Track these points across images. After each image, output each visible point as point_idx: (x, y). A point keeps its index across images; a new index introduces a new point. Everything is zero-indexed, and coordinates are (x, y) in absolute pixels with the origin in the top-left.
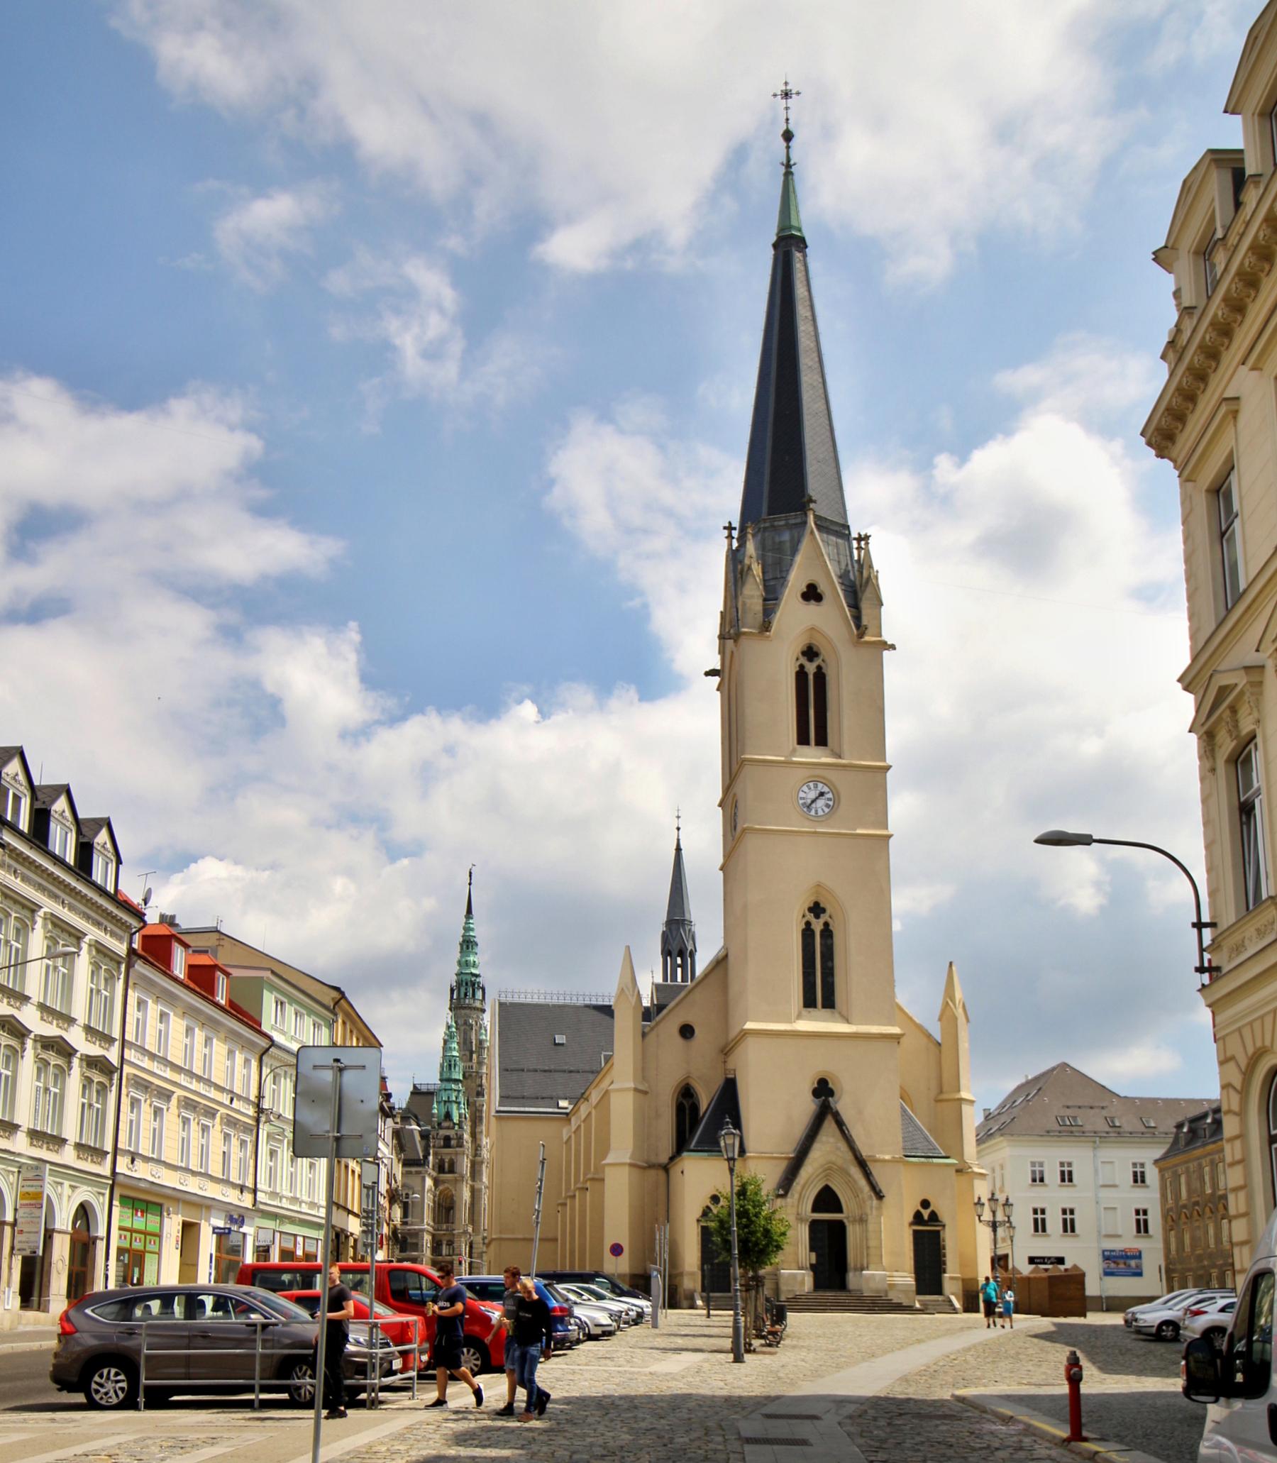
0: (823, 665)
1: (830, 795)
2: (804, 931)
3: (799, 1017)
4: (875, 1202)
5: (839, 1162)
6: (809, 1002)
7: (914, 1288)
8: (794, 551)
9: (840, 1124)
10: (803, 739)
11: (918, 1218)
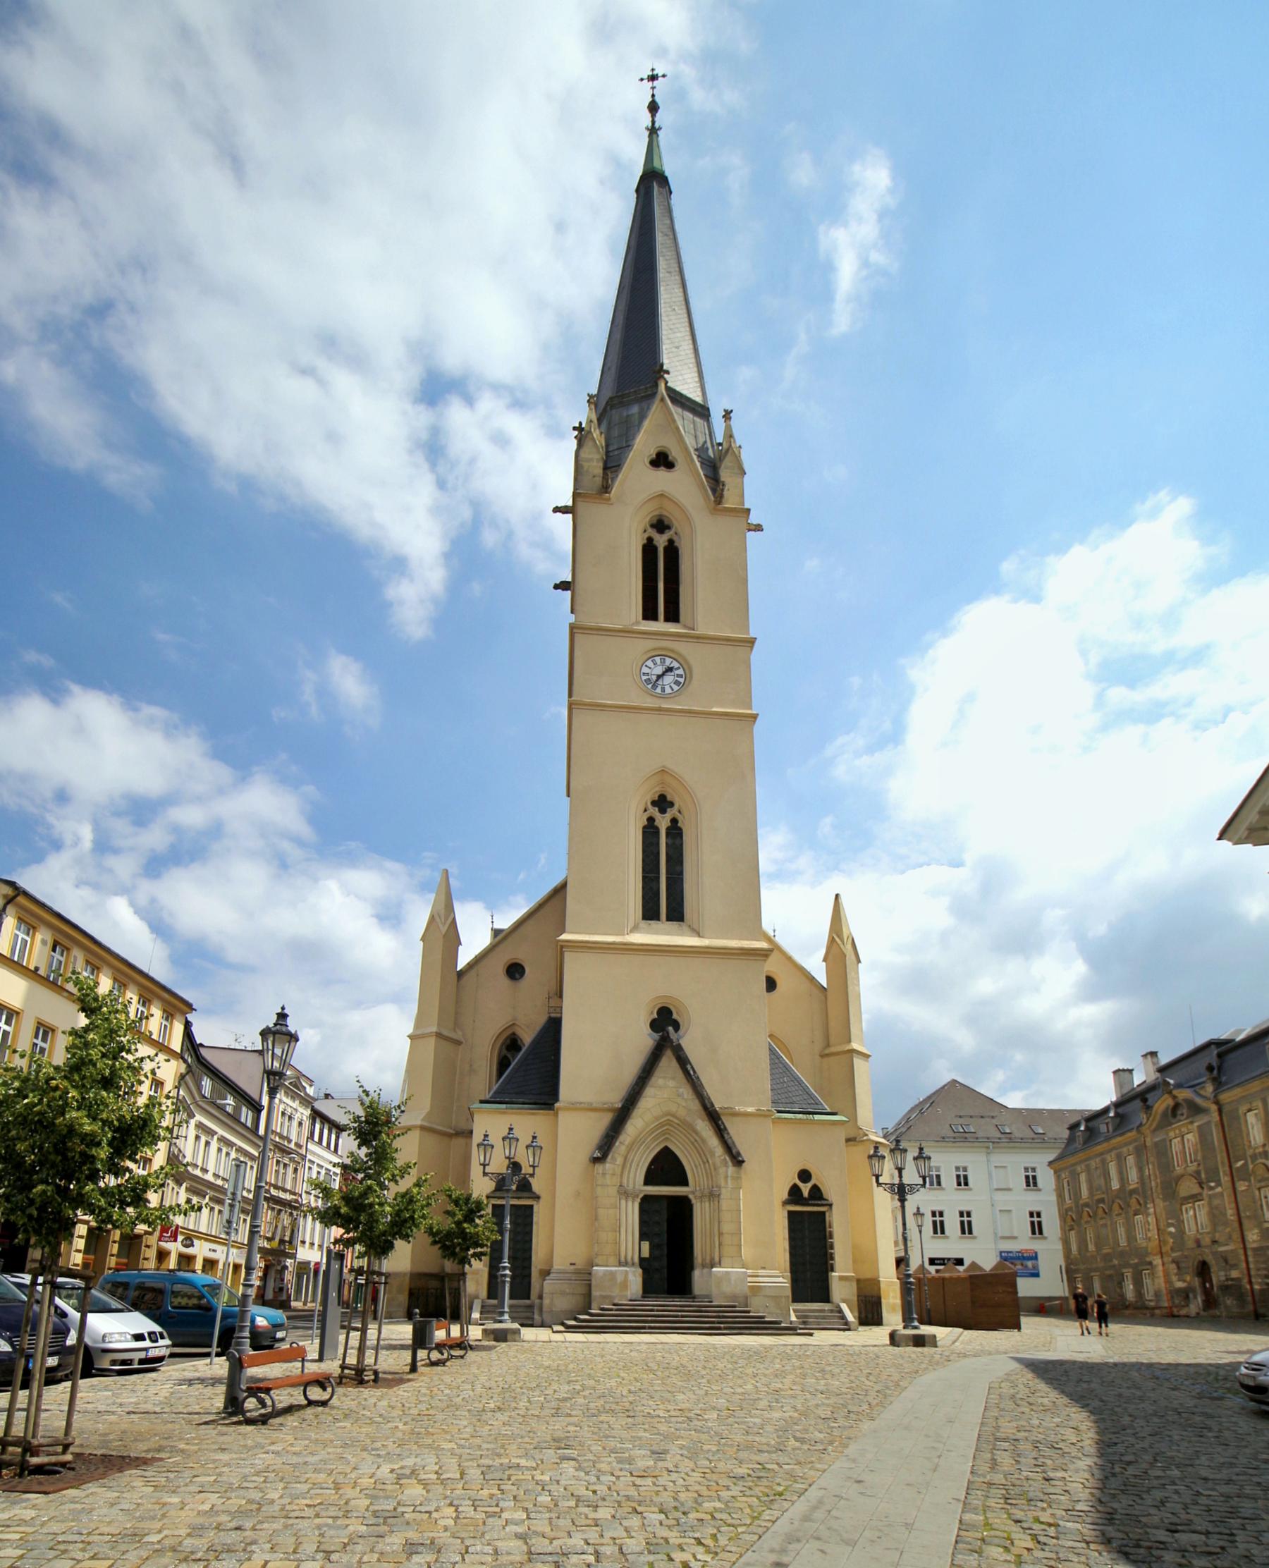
0: (675, 538)
1: (681, 672)
2: (644, 827)
3: (635, 929)
4: (731, 1169)
5: (682, 1113)
6: (650, 913)
7: (789, 1293)
8: (642, 416)
9: (683, 1061)
10: (649, 613)
11: (795, 1193)
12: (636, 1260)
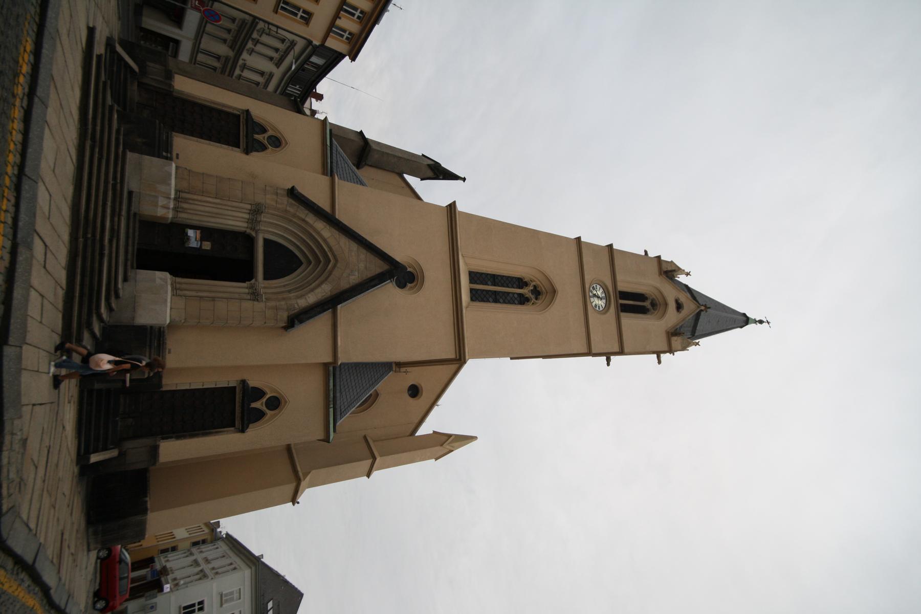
12: (183, 217)
